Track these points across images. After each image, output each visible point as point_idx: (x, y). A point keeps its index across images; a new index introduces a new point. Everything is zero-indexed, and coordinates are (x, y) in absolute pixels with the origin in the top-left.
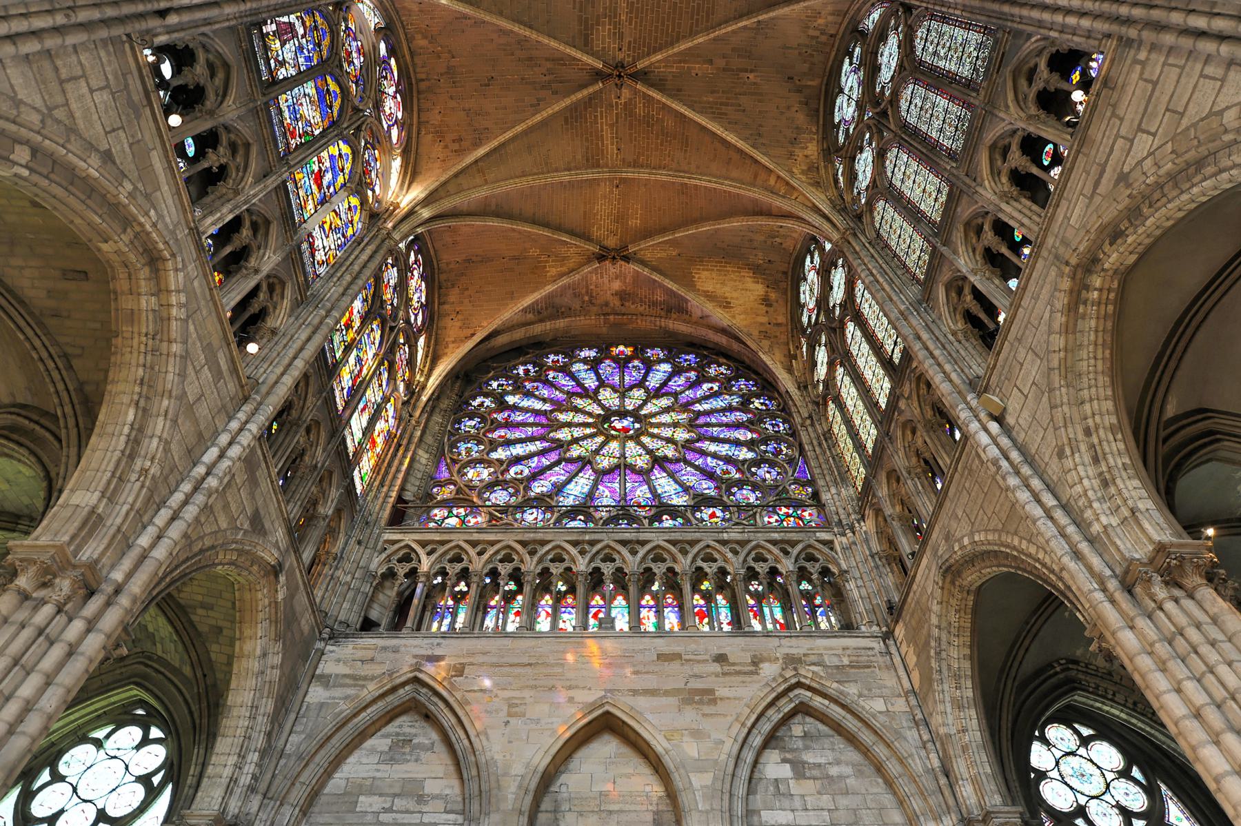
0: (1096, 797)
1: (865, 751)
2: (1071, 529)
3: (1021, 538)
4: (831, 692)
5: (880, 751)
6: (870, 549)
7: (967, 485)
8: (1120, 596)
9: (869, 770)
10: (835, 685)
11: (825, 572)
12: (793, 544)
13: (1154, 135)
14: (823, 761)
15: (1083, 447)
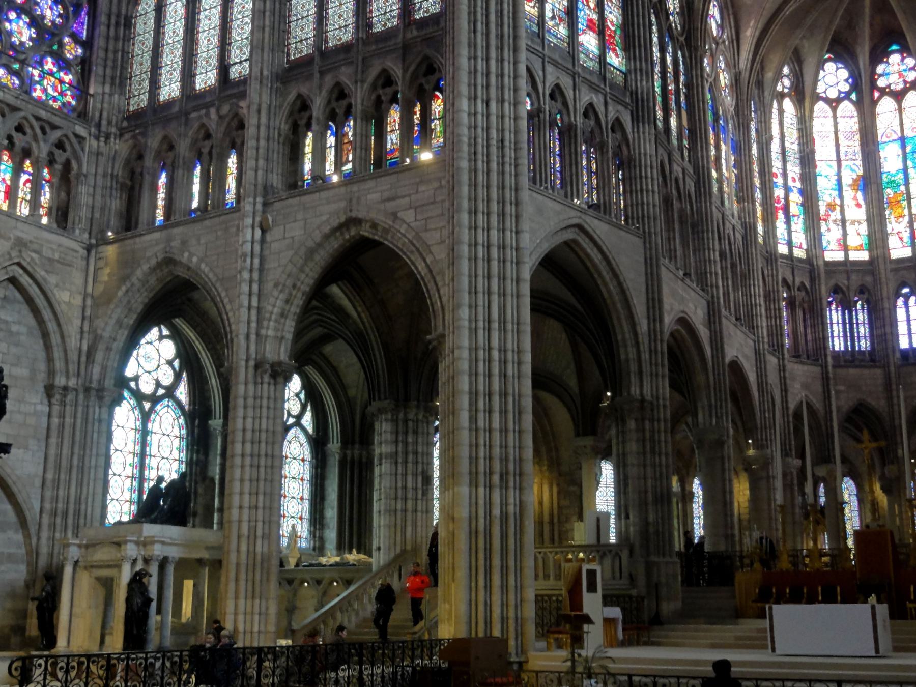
0: (149, 372)
1: (41, 321)
2: (254, 325)
3: (227, 295)
4: (38, 277)
5: (51, 326)
6: (113, 168)
7: (219, 233)
8: (251, 371)
9: (37, 333)
10: (43, 273)
11: (67, 165)
12: (54, 127)
13: (416, 220)
14: (9, 319)
15: (287, 291)
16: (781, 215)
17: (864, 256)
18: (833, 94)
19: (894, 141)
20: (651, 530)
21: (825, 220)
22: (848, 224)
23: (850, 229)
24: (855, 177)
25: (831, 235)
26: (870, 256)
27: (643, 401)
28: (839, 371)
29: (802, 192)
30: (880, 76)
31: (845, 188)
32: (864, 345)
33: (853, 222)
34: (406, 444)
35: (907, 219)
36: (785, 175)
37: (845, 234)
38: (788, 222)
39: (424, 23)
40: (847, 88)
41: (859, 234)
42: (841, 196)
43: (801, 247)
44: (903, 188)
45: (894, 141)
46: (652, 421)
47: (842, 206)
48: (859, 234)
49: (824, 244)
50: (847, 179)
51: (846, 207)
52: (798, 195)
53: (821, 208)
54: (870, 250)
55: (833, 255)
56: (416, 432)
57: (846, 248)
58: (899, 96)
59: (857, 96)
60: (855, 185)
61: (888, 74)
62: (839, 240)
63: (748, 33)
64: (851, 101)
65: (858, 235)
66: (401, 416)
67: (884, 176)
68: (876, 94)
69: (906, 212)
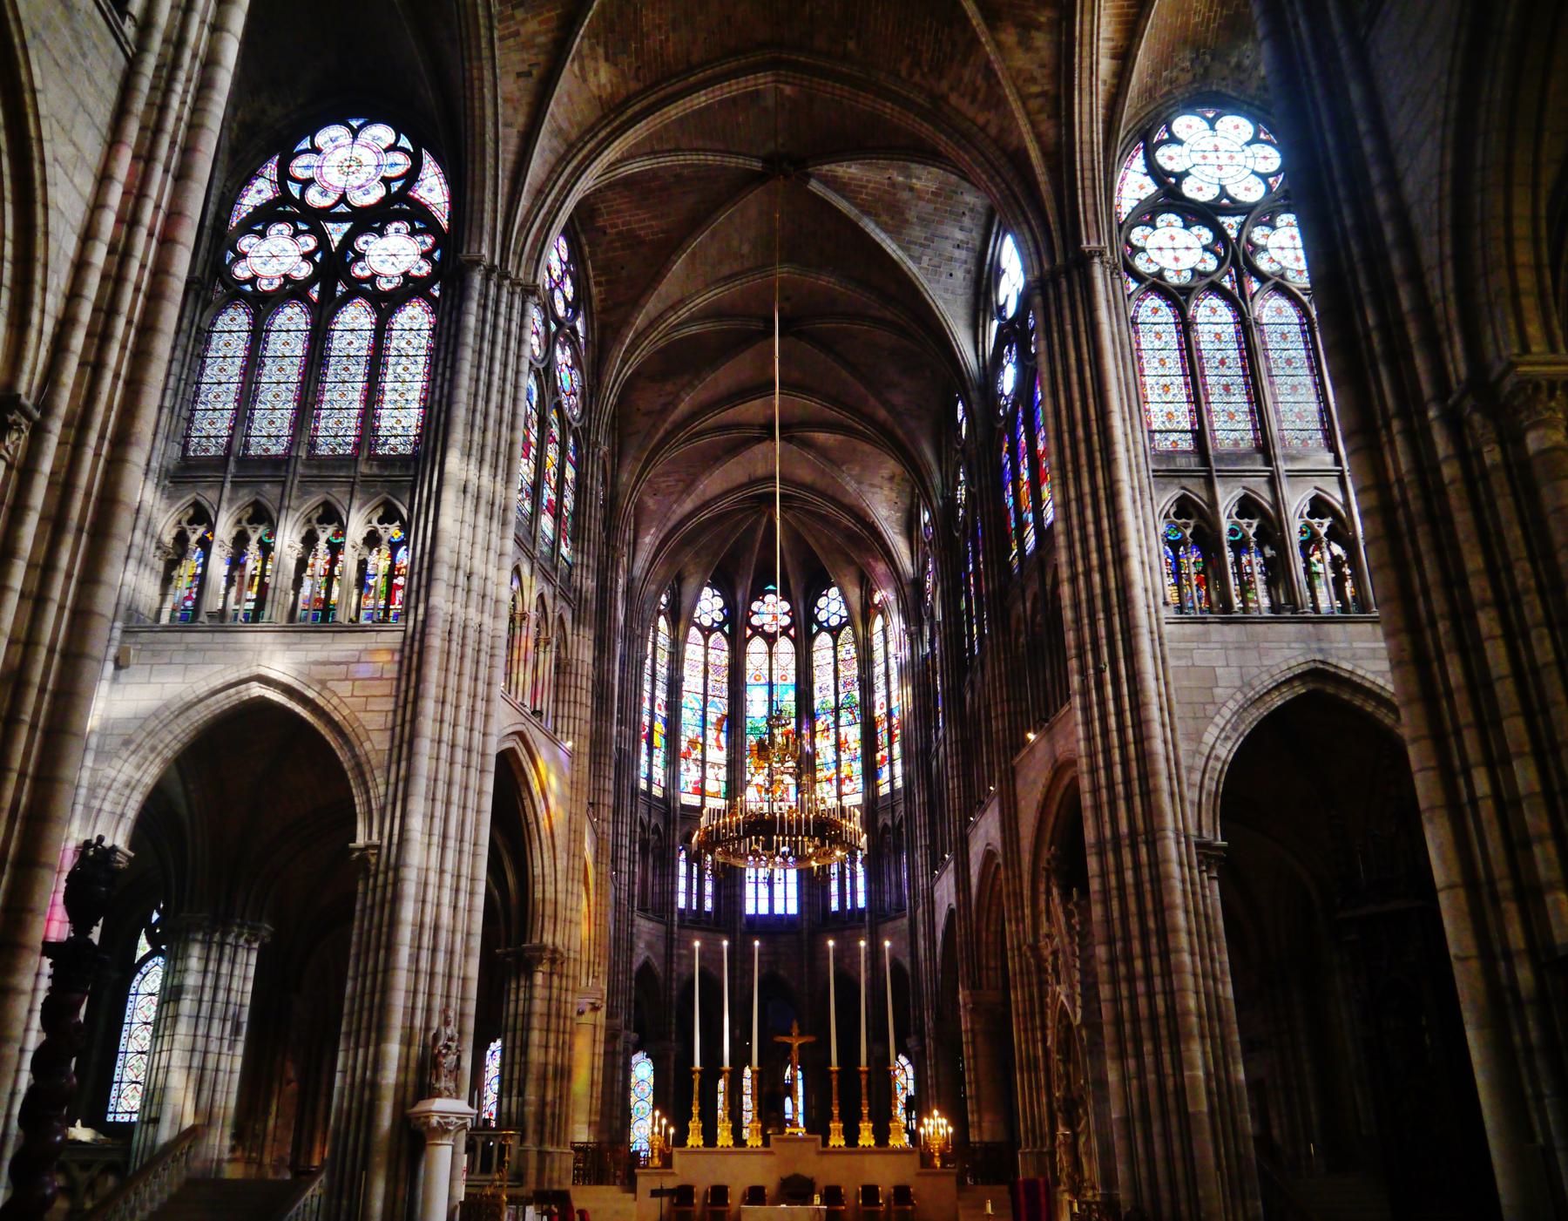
16: (644, 746)
18: (707, 622)
20: (548, 1111)
23: (710, 772)
25: (689, 775)
27: (555, 950)
28: (684, 932)
29: (667, 722)
30: (755, 613)
32: (709, 905)
33: (713, 765)
34: (218, 975)
36: (653, 699)
37: (703, 779)
38: (650, 754)
39: (386, 461)
40: (720, 618)
42: (704, 735)
46: (561, 977)
47: (704, 745)
49: (682, 785)
50: (712, 718)
55: (689, 799)
56: (233, 962)
57: (701, 791)
58: (771, 639)
63: (647, 539)
64: (724, 633)
65: (716, 781)
66: (217, 937)
68: (749, 632)
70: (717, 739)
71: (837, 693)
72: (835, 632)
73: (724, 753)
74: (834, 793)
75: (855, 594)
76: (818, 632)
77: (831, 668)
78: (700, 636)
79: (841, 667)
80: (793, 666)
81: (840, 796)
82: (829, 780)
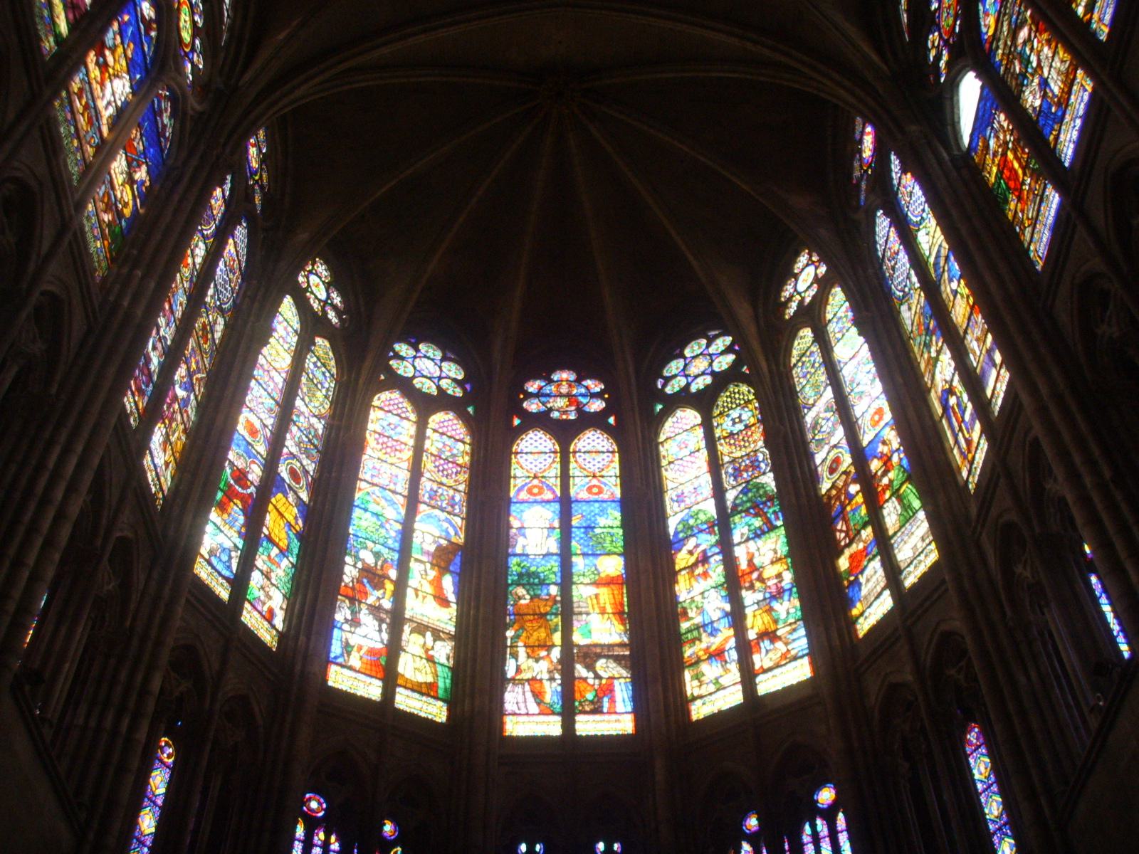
17: (437, 711)
18: (428, 387)
19: (548, 502)
21: (352, 600)
22: (407, 628)
23: (413, 643)
24: (444, 543)
26: (449, 717)
31: (416, 554)
33: (421, 629)
35: (556, 653)
37: (394, 648)
41: (430, 659)
43: (269, 617)
44: (554, 590)
45: (548, 502)
48: (430, 659)
49: (336, 649)
51: (410, 592)
52: (295, 510)
53: (347, 569)
54: (452, 701)
55: (350, 679)
58: (564, 433)
59: (475, 411)
60: (442, 558)
61: (548, 395)
62: (371, 651)
64: (462, 415)
67: (513, 561)
68: (517, 422)
69: (557, 638)
70: (437, 583)
71: (719, 492)
72: (704, 402)
73: (453, 610)
74: (734, 674)
75: (744, 311)
76: (668, 412)
77: (704, 455)
78: (406, 405)
79: (723, 448)
80: (615, 468)
81: (748, 676)
82: (718, 655)
